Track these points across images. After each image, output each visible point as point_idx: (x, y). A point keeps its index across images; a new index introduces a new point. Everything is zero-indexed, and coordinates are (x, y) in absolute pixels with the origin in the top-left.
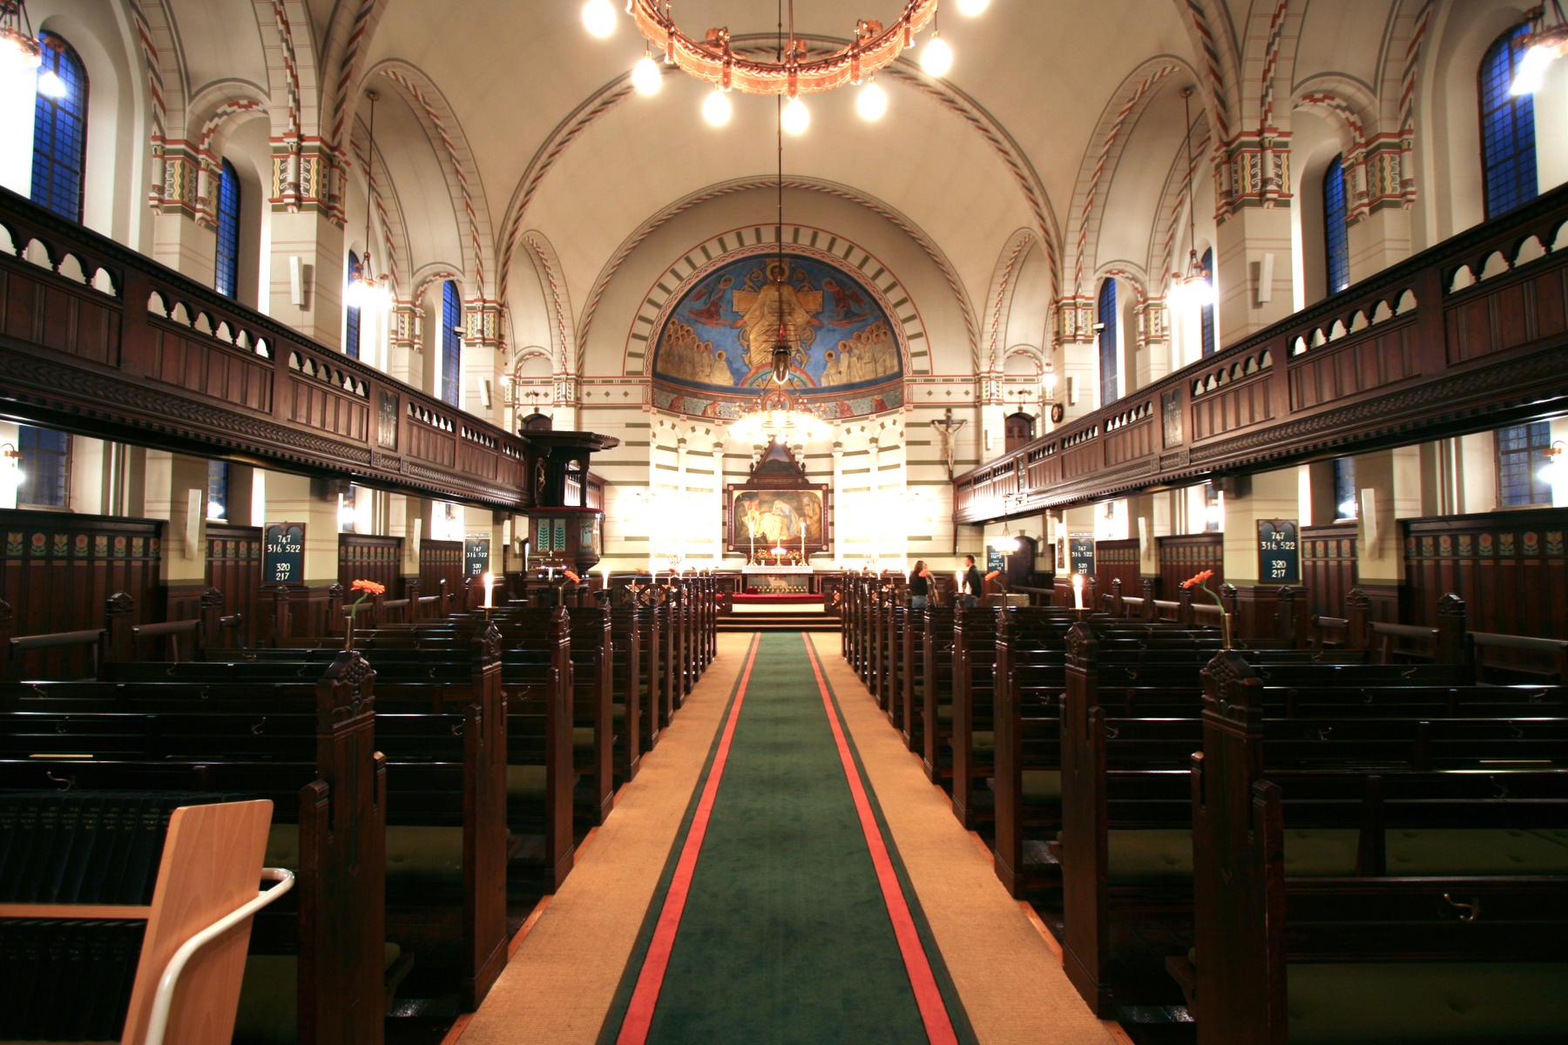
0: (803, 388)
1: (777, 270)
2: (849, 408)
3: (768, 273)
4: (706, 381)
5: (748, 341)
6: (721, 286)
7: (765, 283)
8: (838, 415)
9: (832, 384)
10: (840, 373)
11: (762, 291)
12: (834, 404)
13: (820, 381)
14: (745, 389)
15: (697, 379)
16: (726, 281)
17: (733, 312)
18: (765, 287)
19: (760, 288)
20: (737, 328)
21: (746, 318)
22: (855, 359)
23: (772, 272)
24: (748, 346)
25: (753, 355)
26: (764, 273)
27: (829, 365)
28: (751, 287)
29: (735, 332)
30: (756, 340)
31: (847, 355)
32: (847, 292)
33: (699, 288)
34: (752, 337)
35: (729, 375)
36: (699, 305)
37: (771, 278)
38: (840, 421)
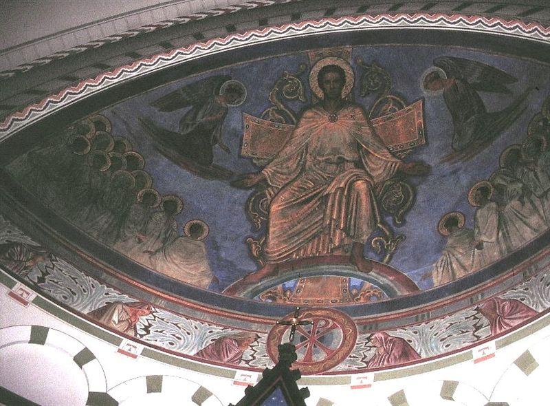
0: (386, 298)
1: (330, 76)
2: (516, 305)
3: (314, 83)
4: (143, 261)
5: (268, 217)
6: (219, 100)
7: (307, 108)
8: (483, 333)
9: (460, 274)
10: (480, 246)
11: (303, 121)
12: (471, 312)
13: (427, 276)
14: (240, 302)
15: (118, 247)
16: (230, 90)
17: (240, 157)
18: (309, 114)
19: (299, 116)
20: (247, 189)
21: (267, 172)
22: (515, 203)
23: (321, 86)
24: (266, 225)
25: (271, 242)
26: (306, 83)
27: (450, 241)
28: (280, 112)
29: (241, 195)
30: (283, 214)
31: (494, 205)
32: (471, 80)
33: (175, 85)
34: (274, 208)
35: (204, 266)
36: (168, 120)
37: (320, 94)
38: (492, 344)
